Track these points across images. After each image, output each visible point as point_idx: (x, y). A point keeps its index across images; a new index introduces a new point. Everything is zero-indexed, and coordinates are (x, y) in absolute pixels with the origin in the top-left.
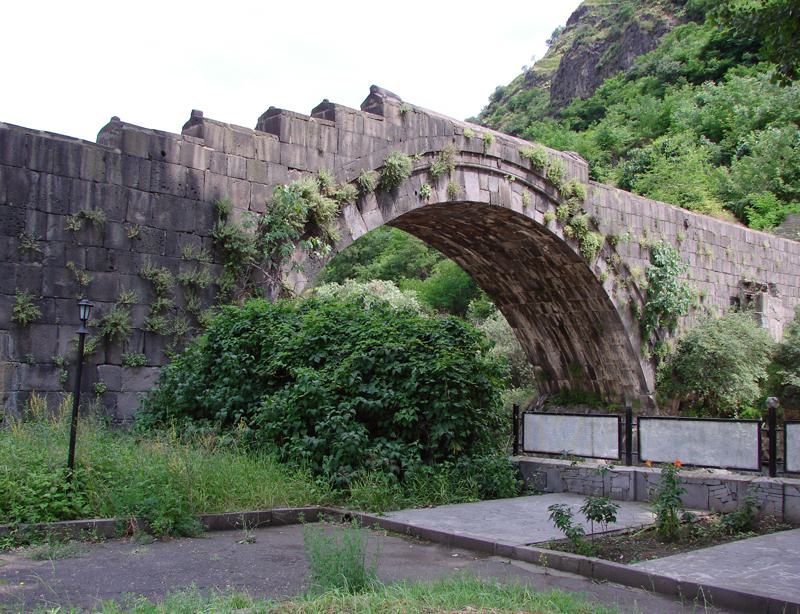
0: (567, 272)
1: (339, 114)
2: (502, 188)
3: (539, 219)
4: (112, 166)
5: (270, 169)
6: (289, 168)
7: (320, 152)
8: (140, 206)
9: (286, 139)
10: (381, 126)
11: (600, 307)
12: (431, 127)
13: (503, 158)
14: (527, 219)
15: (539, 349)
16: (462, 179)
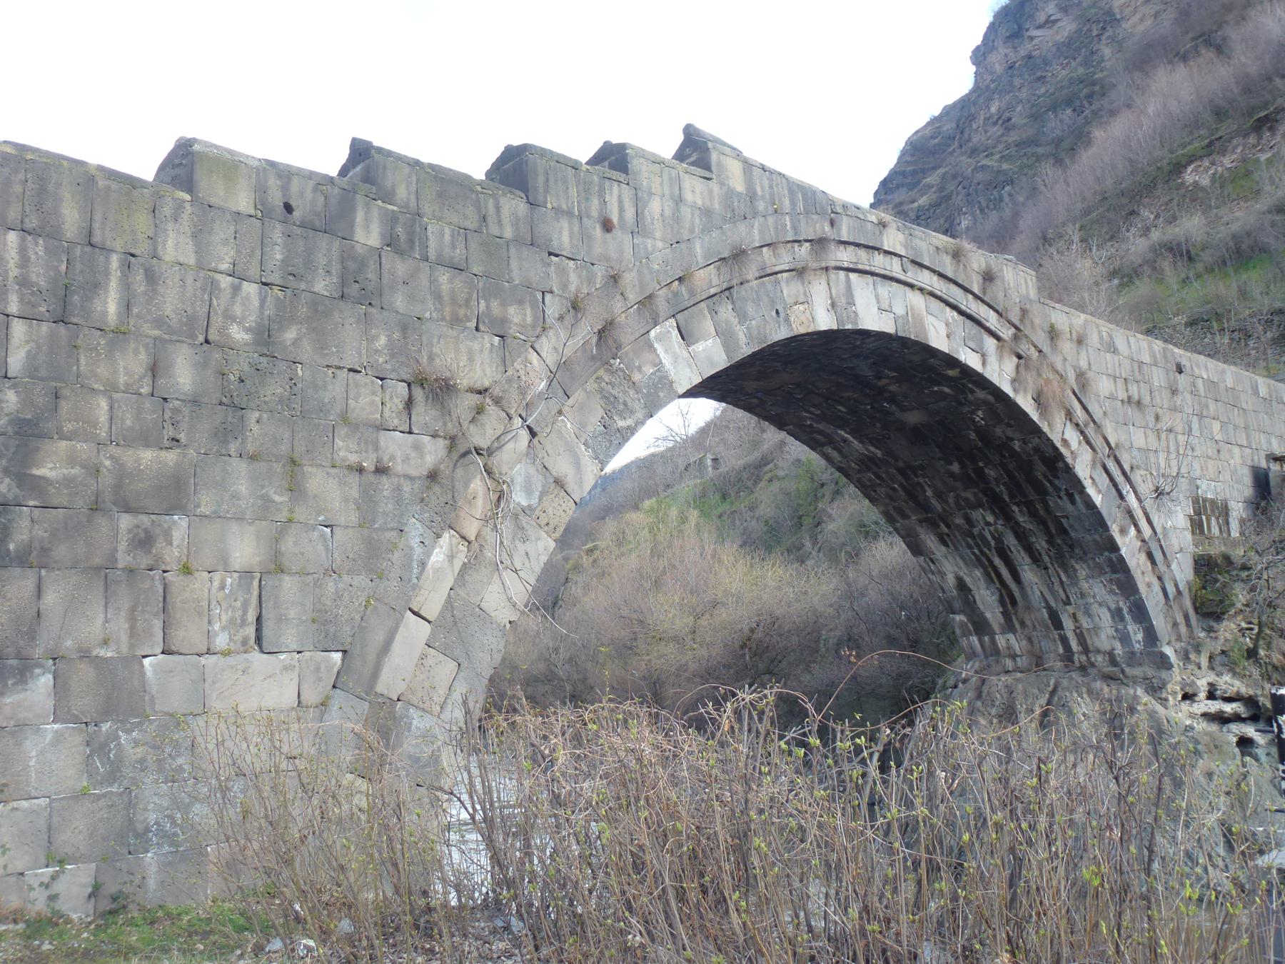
0: (1013, 453)
1: (635, 162)
2: (912, 309)
3: (971, 360)
4: (170, 226)
5: (513, 251)
6: (550, 254)
7: (607, 226)
8: (237, 310)
9: (540, 198)
10: (711, 192)
11: (1070, 507)
12: (793, 204)
14: (952, 361)
15: (962, 585)
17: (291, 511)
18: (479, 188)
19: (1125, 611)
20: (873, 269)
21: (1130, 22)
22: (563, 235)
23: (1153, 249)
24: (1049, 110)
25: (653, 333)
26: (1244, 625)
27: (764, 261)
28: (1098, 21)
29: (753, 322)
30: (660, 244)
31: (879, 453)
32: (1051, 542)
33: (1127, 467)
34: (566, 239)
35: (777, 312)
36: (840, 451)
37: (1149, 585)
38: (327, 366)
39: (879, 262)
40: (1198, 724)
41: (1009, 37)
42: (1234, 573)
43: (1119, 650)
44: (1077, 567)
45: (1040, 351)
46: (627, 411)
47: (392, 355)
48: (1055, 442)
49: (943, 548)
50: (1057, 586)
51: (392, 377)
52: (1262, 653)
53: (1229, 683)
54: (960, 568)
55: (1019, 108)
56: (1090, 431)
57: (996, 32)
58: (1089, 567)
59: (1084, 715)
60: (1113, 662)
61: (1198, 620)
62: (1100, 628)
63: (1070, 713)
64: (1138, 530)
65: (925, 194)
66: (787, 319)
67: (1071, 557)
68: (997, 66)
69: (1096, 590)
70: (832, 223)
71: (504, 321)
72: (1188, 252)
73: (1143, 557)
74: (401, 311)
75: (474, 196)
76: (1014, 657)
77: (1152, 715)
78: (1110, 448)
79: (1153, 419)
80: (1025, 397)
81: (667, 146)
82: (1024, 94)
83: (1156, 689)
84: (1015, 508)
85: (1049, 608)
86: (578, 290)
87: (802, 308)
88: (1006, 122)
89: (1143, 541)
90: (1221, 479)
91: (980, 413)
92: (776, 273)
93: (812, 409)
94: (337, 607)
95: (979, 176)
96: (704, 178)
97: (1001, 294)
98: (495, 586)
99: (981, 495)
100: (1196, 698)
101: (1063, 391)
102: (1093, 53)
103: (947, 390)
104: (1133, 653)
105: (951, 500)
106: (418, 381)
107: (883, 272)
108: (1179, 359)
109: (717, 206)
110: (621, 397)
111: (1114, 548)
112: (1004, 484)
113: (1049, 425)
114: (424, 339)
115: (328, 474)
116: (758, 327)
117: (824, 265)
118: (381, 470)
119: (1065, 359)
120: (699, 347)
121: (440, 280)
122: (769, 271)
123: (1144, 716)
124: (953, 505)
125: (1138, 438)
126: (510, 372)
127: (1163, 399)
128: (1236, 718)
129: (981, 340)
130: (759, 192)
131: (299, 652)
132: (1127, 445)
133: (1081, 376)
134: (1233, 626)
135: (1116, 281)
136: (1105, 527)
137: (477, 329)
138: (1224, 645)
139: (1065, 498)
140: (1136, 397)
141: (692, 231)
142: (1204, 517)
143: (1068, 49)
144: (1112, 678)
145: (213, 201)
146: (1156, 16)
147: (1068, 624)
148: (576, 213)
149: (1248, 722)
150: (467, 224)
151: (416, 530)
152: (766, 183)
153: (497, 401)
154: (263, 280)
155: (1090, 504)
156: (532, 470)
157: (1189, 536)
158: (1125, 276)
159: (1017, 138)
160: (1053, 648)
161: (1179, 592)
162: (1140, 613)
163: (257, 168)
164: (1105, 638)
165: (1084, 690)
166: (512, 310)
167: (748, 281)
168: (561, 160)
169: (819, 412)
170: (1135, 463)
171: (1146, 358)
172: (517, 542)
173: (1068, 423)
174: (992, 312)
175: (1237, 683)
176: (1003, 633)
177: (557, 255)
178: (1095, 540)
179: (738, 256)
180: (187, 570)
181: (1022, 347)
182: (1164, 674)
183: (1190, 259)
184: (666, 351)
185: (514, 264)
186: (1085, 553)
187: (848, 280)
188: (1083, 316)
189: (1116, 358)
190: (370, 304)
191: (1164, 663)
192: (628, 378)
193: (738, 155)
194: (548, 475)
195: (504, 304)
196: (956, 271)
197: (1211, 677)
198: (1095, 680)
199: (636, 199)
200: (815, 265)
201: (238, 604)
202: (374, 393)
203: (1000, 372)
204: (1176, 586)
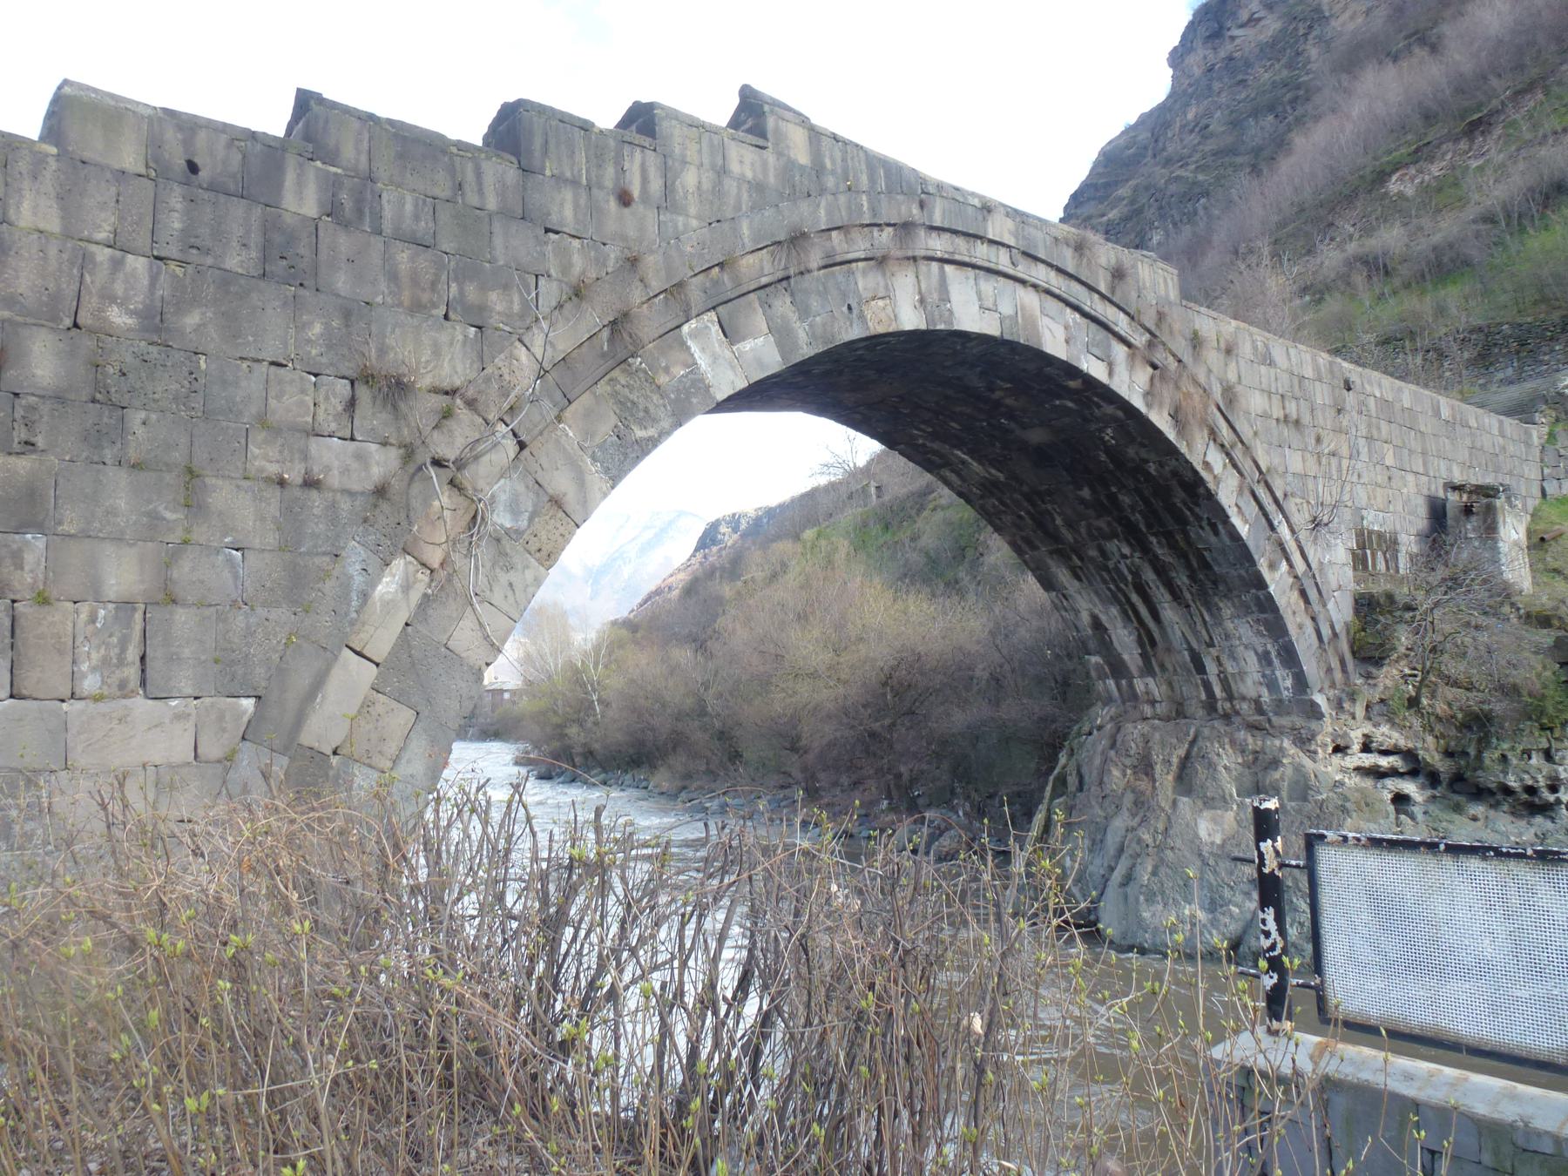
1: (665, 124)
3: (1096, 370)
4: (26, 184)
5: (497, 227)
6: (547, 230)
7: (625, 199)
8: (119, 289)
10: (765, 164)
11: (1213, 539)
13: (1022, 245)
14: (1072, 371)
15: (1097, 624)
16: (943, 281)
17: (188, 531)
18: (454, 150)
19: (1273, 654)
20: (974, 261)
21: (1341, 19)
22: (564, 208)
23: (1350, 263)
24: (1249, 116)
25: (685, 328)
26: (1407, 671)
27: (833, 247)
28: (1305, 19)
29: (818, 319)
30: (694, 223)
31: (1001, 477)
32: (1192, 577)
33: (1279, 494)
34: (568, 212)
35: (850, 308)
36: (958, 474)
37: (1300, 627)
38: (241, 358)
39: (982, 253)
40: (1350, 779)
41: (1209, 37)
42: (1398, 613)
43: (1266, 697)
44: (1221, 605)
45: (1180, 361)
46: (648, 418)
47: (330, 347)
48: (1195, 464)
49: (1076, 583)
50: (1200, 627)
51: (328, 372)
52: (1425, 701)
53: (1386, 734)
54: (1095, 605)
55: (1218, 114)
56: (1238, 453)
57: (1195, 31)
58: (1234, 607)
59: (1226, 768)
60: (1259, 709)
61: (1356, 666)
62: (1245, 673)
63: (1211, 766)
64: (1291, 565)
65: (1116, 207)
66: (862, 317)
67: (1215, 594)
68: (1195, 68)
69: (1242, 631)
70: (922, 205)
71: (482, 308)
72: (1385, 266)
73: (1295, 595)
74: (343, 294)
75: (446, 159)
76: (1153, 703)
77: (1298, 768)
78: (1261, 472)
79: (1313, 442)
80: (1160, 413)
81: (719, 110)
82: (1223, 99)
83: (1304, 741)
84: (1154, 540)
85: (1191, 650)
86: (583, 273)
87: (881, 303)
88: (1203, 130)
89: (1296, 577)
90: (1391, 508)
91: (1109, 431)
92: (850, 262)
93: (923, 426)
94: (248, 645)
95: (1173, 188)
96: (757, 146)
97: (1134, 295)
98: (468, 623)
99: (1115, 524)
100: (1349, 751)
101: (1206, 407)
102: (1298, 54)
103: (1070, 404)
104: (1281, 701)
105: (1083, 531)
106: (365, 377)
107: (986, 264)
108: (1348, 375)
109: (772, 180)
110: (642, 402)
111: (1261, 584)
112: (1140, 512)
113: (1188, 445)
114: (374, 328)
115: (238, 487)
116: (824, 325)
117: (910, 254)
118: (310, 483)
119: (1210, 371)
120: (747, 346)
121: (399, 257)
122: (838, 259)
123: (1289, 771)
124: (1085, 536)
125: (1295, 462)
126: (489, 370)
127: (1326, 419)
128: (1393, 773)
129: (1109, 346)
130: (829, 165)
131: (196, 698)
132: (1281, 469)
133: (1229, 393)
134: (1395, 672)
135: (1308, 298)
136: (1252, 562)
137: (446, 317)
138: (1383, 693)
139: (1207, 528)
140: (1294, 416)
141: (738, 208)
142: (1368, 552)
143: (1271, 50)
144: (1257, 728)
145: (87, 155)
146: (1368, 12)
147: (1212, 669)
148: (584, 181)
149: (1406, 777)
150: (437, 192)
151: (355, 556)
152: (838, 155)
153: (471, 404)
154: (155, 253)
155: (1235, 535)
156: (521, 488)
157: (1349, 572)
158: (1315, 292)
159: (1215, 147)
160: (1195, 694)
161: (1335, 635)
162: (1289, 656)
163: (149, 117)
164: (1251, 684)
165: (1227, 740)
166: (493, 296)
167: (809, 271)
168: (566, 119)
169: (930, 430)
170: (1289, 489)
171: (1309, 372)
172: (498, 570)
173: (1212, 443)
174: (1122, 315)
175: (1396, 735)
176: (1141, 676)
177: (557, 232)
178: (1240, 576)
179: (797, 239)
180: (43, 600)
181: (1158, 356)
182: (1314, 725)
183: (1387, 273)
184: (703, 350)
185: (498, 241)
186: (1230, 590)
187: (942, 274)
188: (1234, 323)
189: (1272, 371)
190: (301, 285)
191: (1314, 712)
192: (653, 382)
193: (803, 121)
194: (541, 492)
195: (484, 288)
196: (1079, 266)
197: (1367, 728)
198: (1239, 730)
199: (666, 172)
200: (899, 254)
201: (115, 640)
202: (303, 391)
203: (1130, 384)
204: (1332, 627)
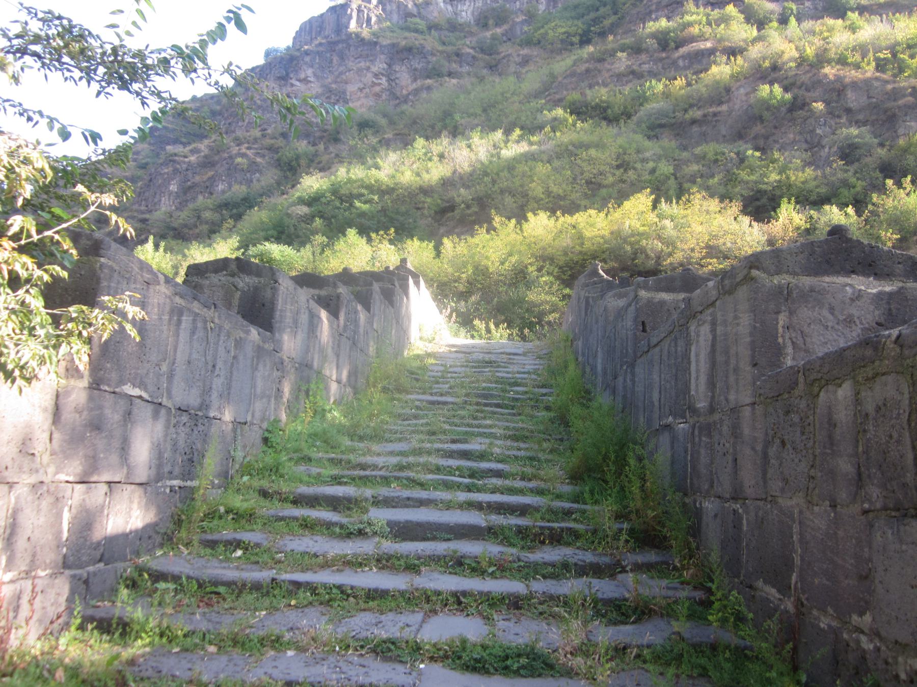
28: (336, 95)
57: (271, 69)
